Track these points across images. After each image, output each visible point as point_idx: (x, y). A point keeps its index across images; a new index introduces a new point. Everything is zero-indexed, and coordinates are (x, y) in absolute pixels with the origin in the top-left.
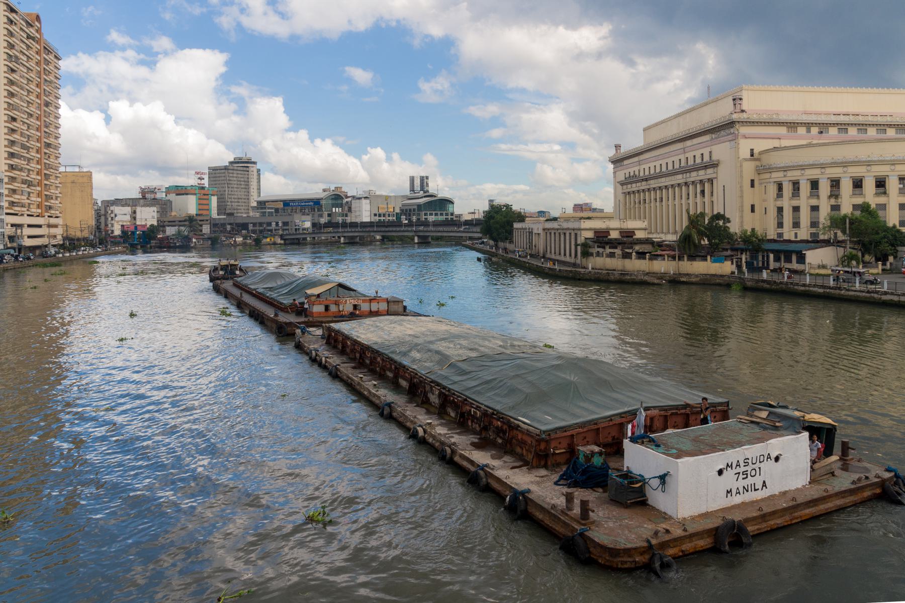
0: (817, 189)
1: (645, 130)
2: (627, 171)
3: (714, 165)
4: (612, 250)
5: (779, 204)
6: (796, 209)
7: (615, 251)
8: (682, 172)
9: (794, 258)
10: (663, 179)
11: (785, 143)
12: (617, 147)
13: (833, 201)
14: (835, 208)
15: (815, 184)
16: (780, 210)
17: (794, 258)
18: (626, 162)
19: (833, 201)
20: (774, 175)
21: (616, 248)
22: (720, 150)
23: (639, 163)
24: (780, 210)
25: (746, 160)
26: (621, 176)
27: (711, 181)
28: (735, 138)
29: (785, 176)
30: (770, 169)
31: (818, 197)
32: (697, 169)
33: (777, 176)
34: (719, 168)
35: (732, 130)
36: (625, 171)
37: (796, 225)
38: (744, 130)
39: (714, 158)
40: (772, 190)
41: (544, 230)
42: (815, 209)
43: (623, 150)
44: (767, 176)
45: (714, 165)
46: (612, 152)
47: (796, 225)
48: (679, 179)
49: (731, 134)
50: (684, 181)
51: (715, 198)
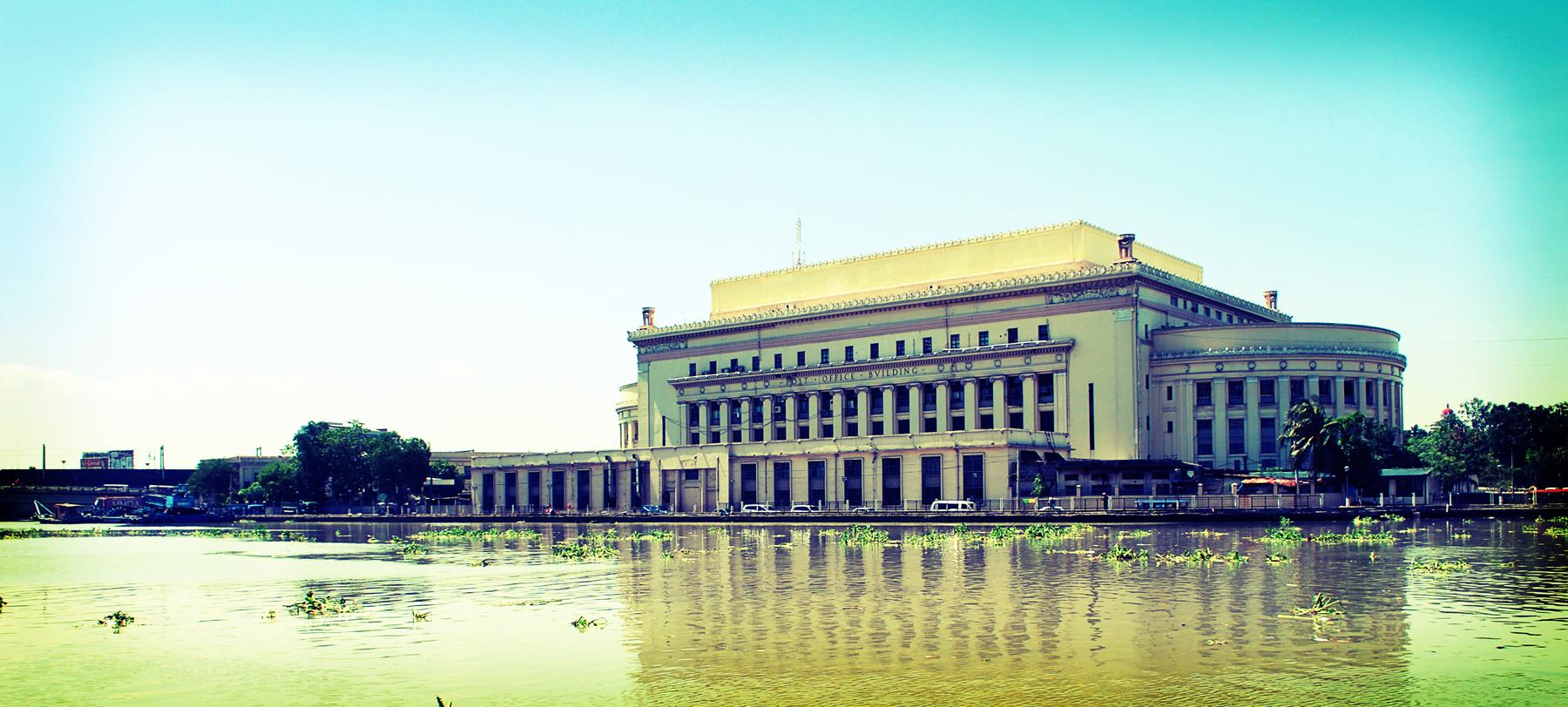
0: (1272, 393)
2: (702, 363)
3: (1068, 348)
4: (1132, 482)
5: (1203, 414)
7: (1140, 482)
8: (940, 362)
10: (857, 375)
12: (647, 312)
16: (1204, 426)
18: (692, 343)
22: (1061, 327)
23: (759, 345)
24: (1204, 426)
25: (1142, 341)
32: (997, 355)
33: (1202, 370)
34: (1072, 353)
36: (693, 360)
40: (1188, 394)
43: (667, 321)
45: (1068, 348)
46: (636, 324)
48: (928, 373)
50: (948, 375)
51: (1058, 405)
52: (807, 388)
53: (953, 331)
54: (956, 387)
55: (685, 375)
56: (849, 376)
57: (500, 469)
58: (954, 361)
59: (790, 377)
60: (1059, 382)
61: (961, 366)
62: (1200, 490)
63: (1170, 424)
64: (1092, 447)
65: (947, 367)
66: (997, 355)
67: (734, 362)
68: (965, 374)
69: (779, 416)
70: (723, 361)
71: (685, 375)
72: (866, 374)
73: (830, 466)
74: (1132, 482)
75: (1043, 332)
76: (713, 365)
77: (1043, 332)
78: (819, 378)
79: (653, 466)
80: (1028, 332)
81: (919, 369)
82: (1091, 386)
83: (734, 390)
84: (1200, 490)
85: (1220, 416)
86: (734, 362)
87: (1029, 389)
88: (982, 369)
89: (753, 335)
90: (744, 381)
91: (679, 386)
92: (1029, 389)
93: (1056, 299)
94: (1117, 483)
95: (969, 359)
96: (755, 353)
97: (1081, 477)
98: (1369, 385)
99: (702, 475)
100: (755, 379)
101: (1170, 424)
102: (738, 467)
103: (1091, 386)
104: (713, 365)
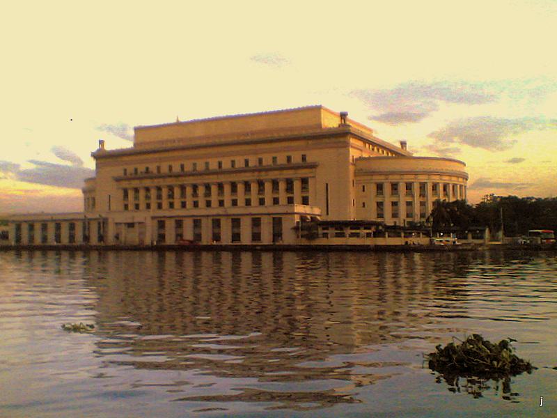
1: (136, 129)
4: (354, 231)
6: (395, 204)
7: (358, 231)
9: (470, 236)
10: (211, 177)
11: (365, 155)
12: (101, 142)
13: (421, 199)
14: (423, 204)
15: (409, 186)
16: (380, 205)
17: (470, 236)
19: (421, 199)
20: (374, 177)
21: (359, 229)
23: (161, 160)
24: (380, 205)
26: (118, 171)
27: (304, 181)
28: (347, 145)
29: (387, 179)
30: (373, 173)
31: (413, 196)
32: (282, 168)
35: (342, 139)
37: (395, 215)
38: (352, 141)
39: (309, 160)
41: (153, 218)
42: (409, 204)
44: (369, 177)
46: (95, 148)
47: (395, 215)
49: (340, 142)
50: (255, 178)
52: (185, 182)
53: (260, 156)
54: (261, 184)
55: (121, 173)
56: (207, 177)
57: (25, 221)
58: (260, 171)
59: (177, 176)
60: (310, 181)
61: (263, 173)
62: (387, 235)
63: (364, 204)
64: (327, 214)
65: (256, 174)
66: (282, 168)
67: (147, 169)
68: (264, 178)
69: (171, 196)
70: (142, 168)
71: (121, 173)
72: (215, 176)
73: (204, 221)
74: (354, 231)
75: (304, 158)
76: (136, 170)
77: (304, 158)
78: (191, 178)
79: (110, 221)
80: (296, 159)
81: (243, 174)
82: (327, 184)
83: (147, 183)
84: (387, 235)
85: (388, 199)
86: (147, 169)
87: (297, 186)
88: (274, 175)
89: (157, 156)
90: (151, 178)
91: (118, 180)
92: (297, 186)
93: (310, 142)
94: (348, 231)
95: (268, 169)
96: (157, 164)
97: (330, 228)
98: (453, 187)
99: (136, 226)
100: (160, 177)
101: (364, 204)
102: (156, 222)
103: (327, 184)
104: (136, 170)
